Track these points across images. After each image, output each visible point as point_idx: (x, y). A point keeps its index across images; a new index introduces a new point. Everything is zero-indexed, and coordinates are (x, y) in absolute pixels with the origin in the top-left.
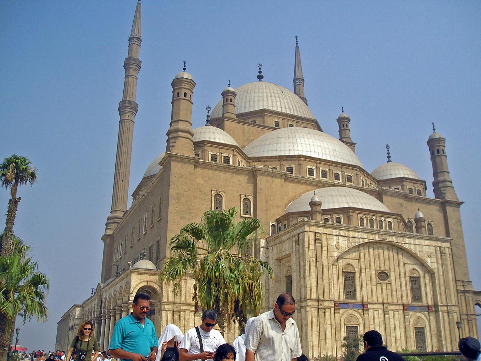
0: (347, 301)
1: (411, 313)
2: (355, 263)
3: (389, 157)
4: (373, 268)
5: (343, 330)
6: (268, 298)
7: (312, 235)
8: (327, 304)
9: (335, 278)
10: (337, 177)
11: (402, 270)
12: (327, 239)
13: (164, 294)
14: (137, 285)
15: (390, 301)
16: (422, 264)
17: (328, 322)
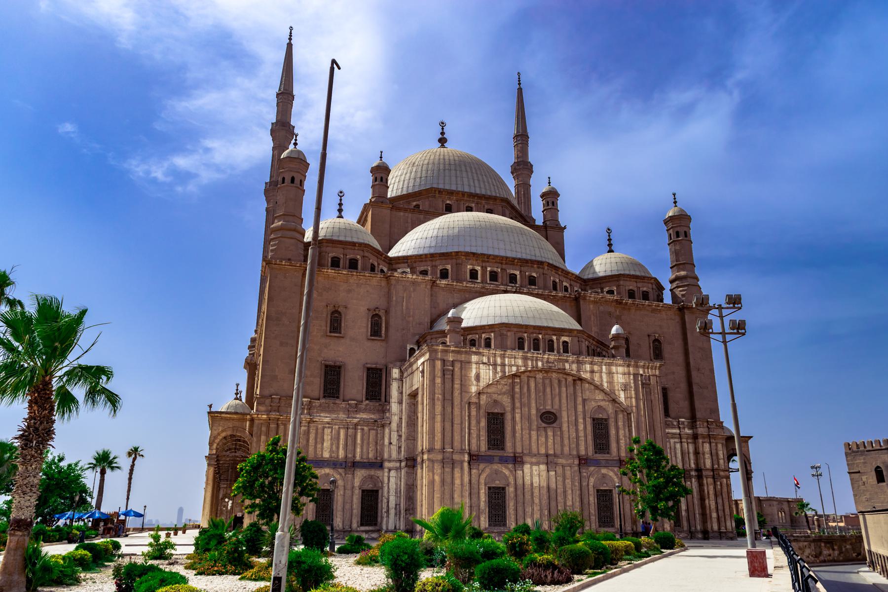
0: (491, 453)
1: (592, 469)
2: (506, 401)
3: (610, 245)
4: (533, 405)
5: (482, 491)
6: (400, 447)
7: (438, 364)
8: (456, 457)
9: (474, 422)
10: (513, 279)
11: (580, 408)
12: (461, 369)
13: (254, 444)
14: (219, 434)
15: (558, 452)
16: (614, 401)
17: (457, 482)
